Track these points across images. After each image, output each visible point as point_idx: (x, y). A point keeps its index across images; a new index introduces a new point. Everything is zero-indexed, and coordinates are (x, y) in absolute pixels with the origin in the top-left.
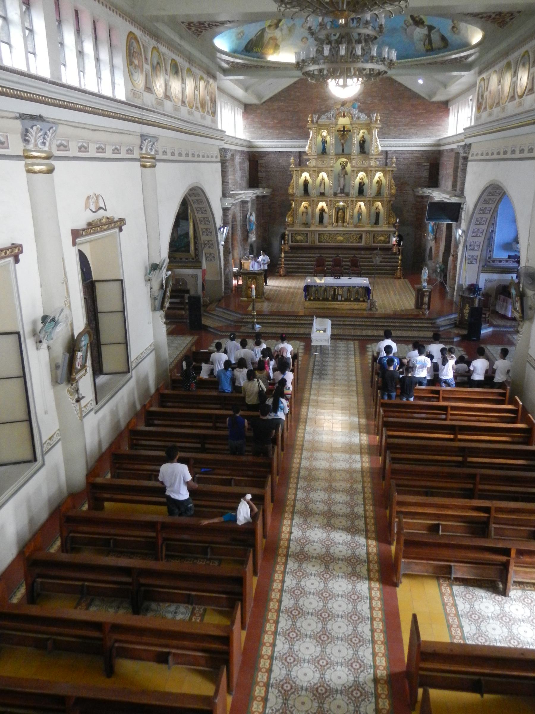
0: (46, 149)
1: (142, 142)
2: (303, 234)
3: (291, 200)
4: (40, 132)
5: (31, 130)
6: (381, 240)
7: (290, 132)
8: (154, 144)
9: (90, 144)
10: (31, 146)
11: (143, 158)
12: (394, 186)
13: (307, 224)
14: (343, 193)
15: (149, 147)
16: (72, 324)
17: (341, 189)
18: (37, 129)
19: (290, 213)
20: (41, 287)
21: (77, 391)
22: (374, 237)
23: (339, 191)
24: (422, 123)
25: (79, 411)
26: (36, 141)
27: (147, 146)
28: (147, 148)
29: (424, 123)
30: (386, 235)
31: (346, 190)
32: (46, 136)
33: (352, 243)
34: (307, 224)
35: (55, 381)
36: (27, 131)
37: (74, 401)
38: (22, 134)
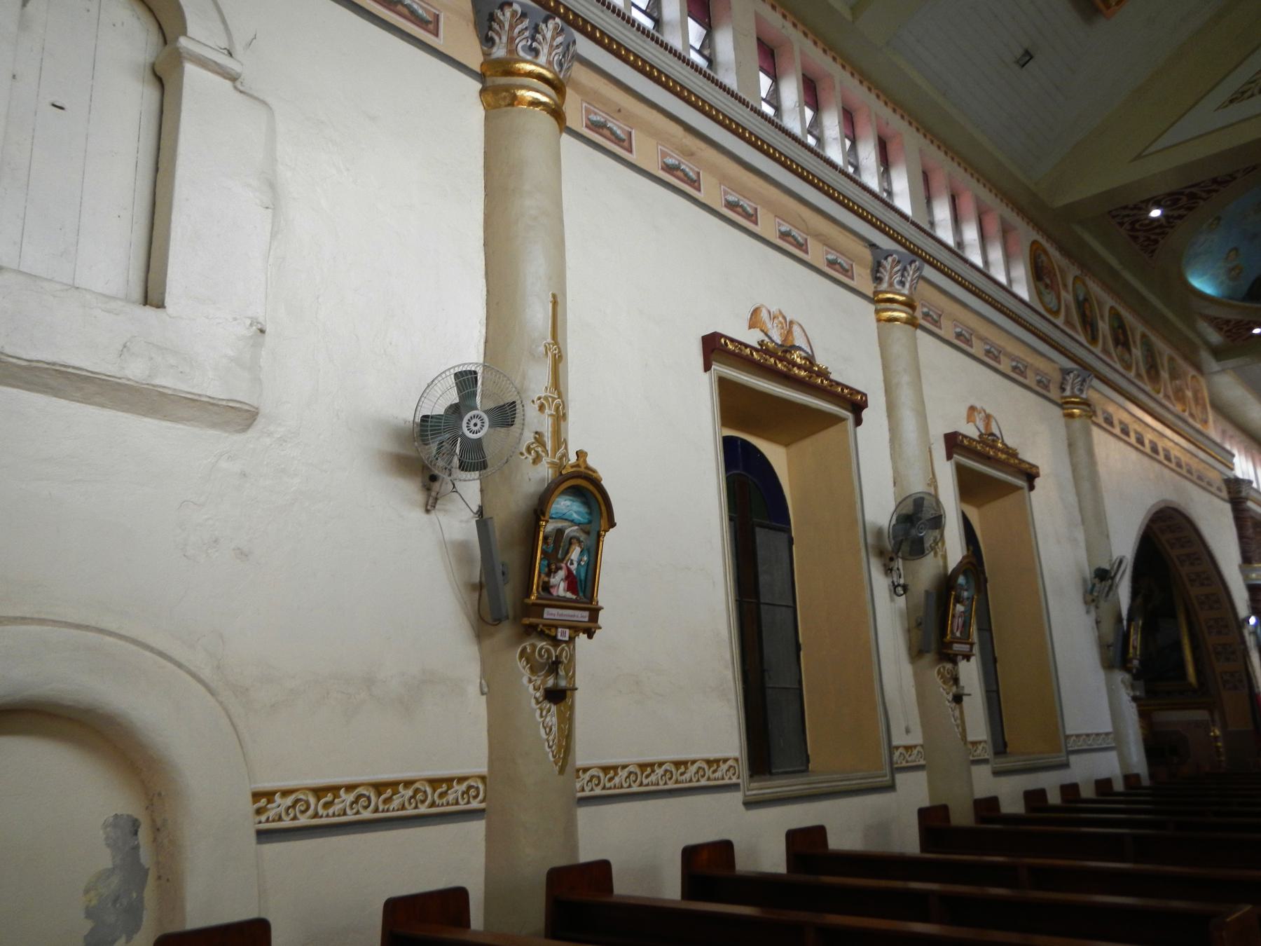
0: (906, 291)
1: (1064, 379)
4: (896, 265)
5: (884, 262)
8: (1084, 380)
9: (973, 337)
10: (884, 286)
11: (1067, 403)
15: (1077, 387)
16: (945, 557)
18: (893, 261)
20: (895, 485)
21: (956, 680)
25: (959, 722)
26: (891, 278)
27: (1072, 383)
28: (1072, 389)
32: (906, 274)
35: (916, 653)
36: (879, 264)
37: (950, 697)
38: (872, 271)
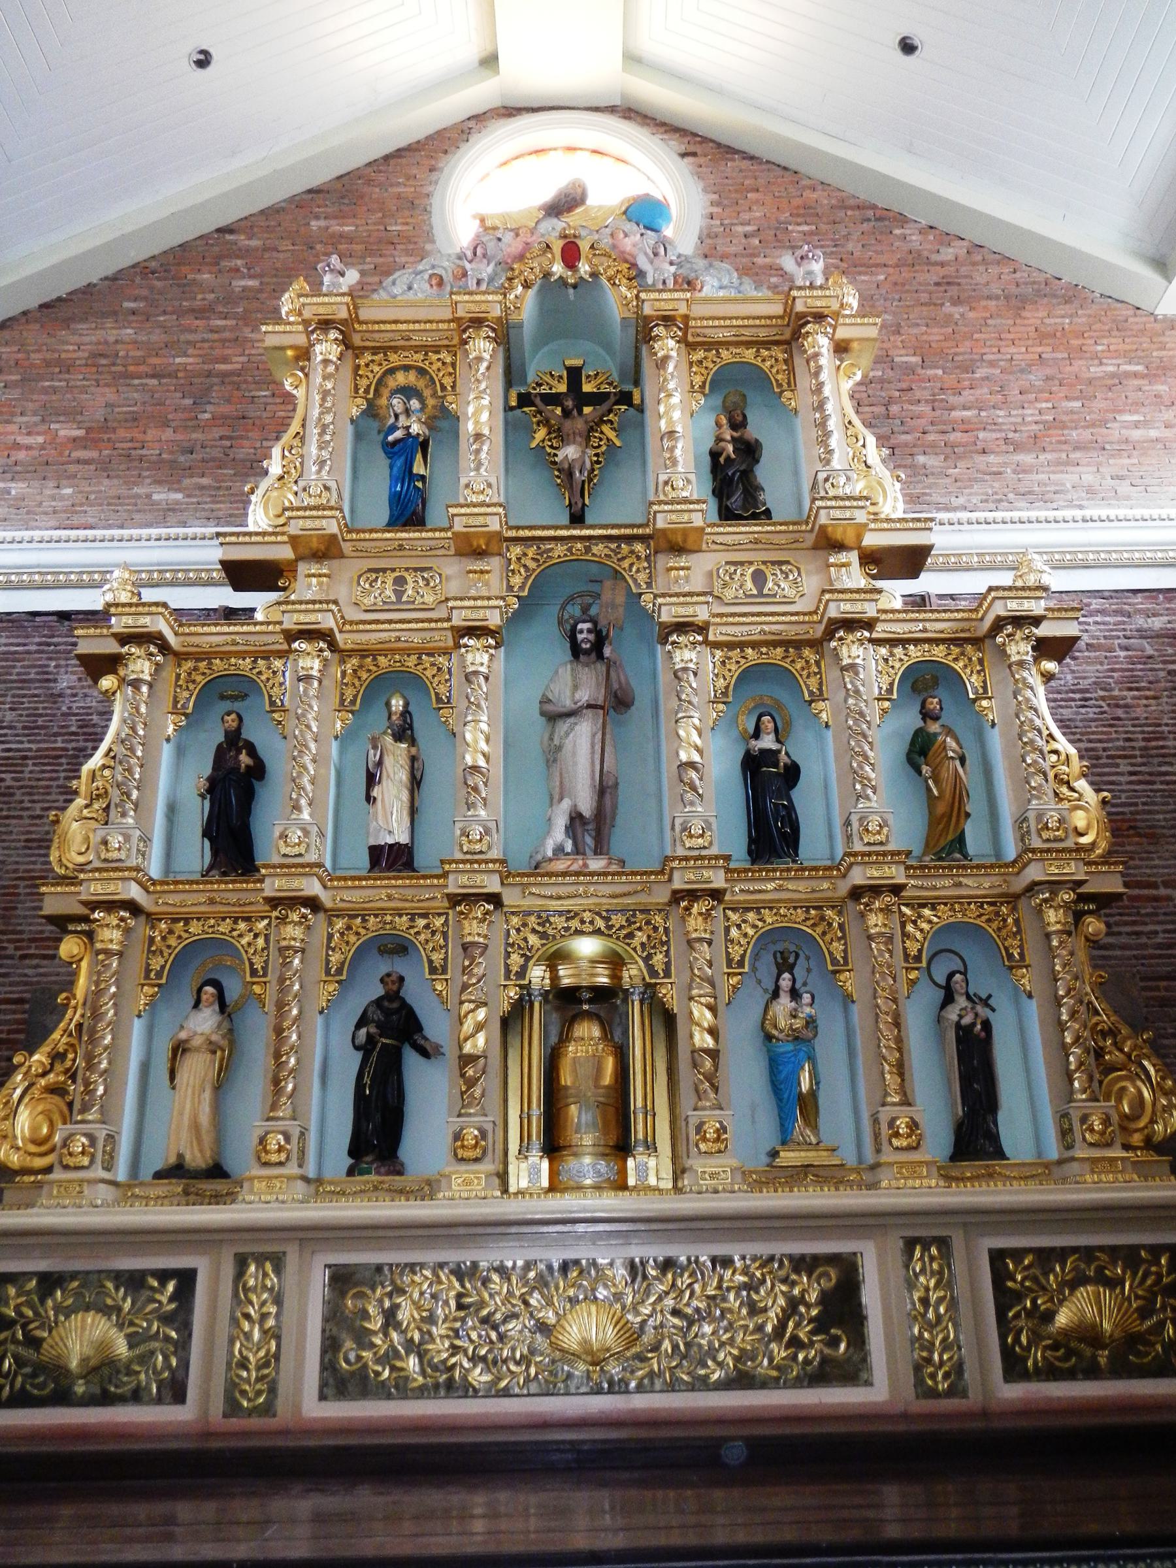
2: (134, 1281)
3: (62, 923)
6: (1087, 1334)
7: (161, 496)
12: (1082, 785)
13: (217, 1171)
14: (598, 851)
17: (576, 820)
19: (40, 1057)
22: (1005, 1298)
23: (559, 834)
24: (1136, 434)
29: (1153, 434)
30: (1129, 1256)
31: (621, 840)
33: (742, 1380)
34: (217, 1171)
